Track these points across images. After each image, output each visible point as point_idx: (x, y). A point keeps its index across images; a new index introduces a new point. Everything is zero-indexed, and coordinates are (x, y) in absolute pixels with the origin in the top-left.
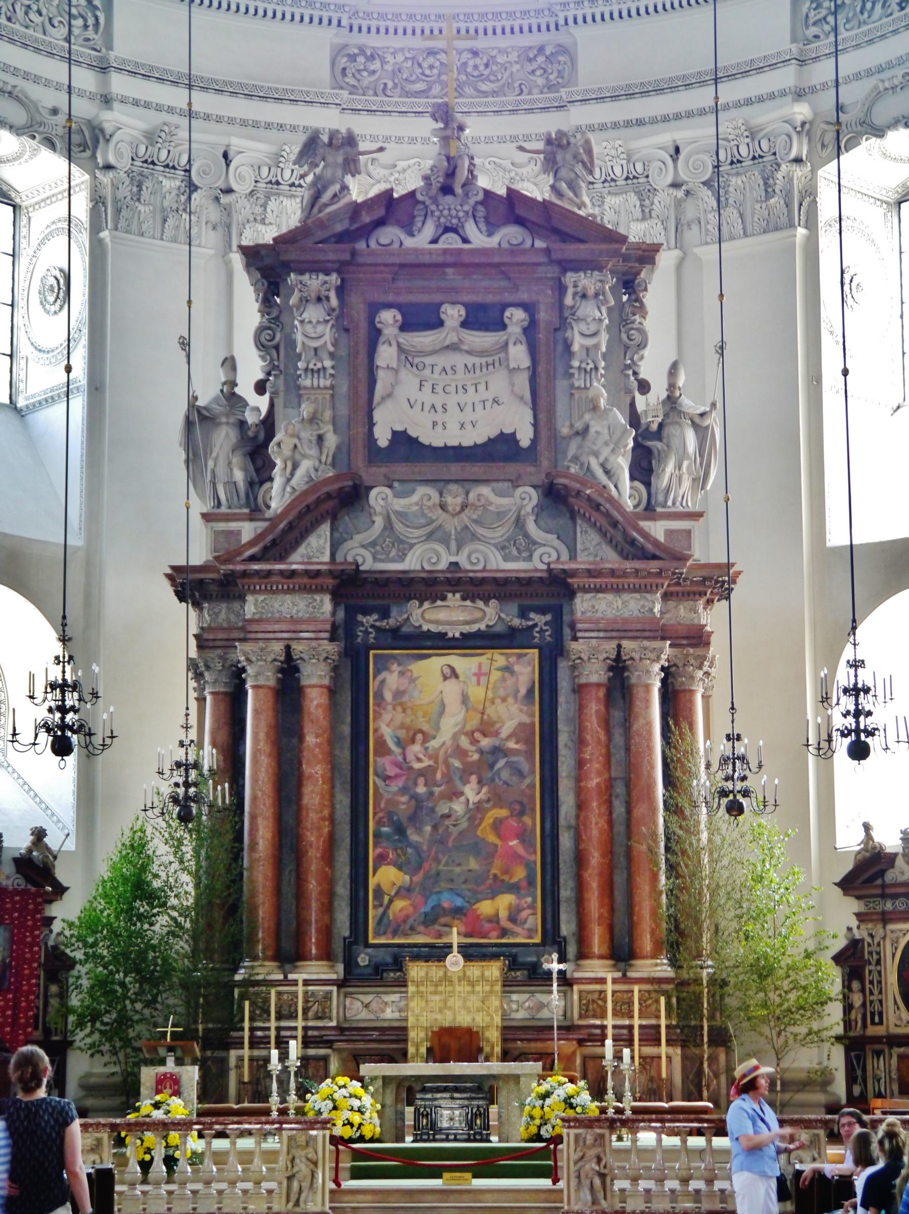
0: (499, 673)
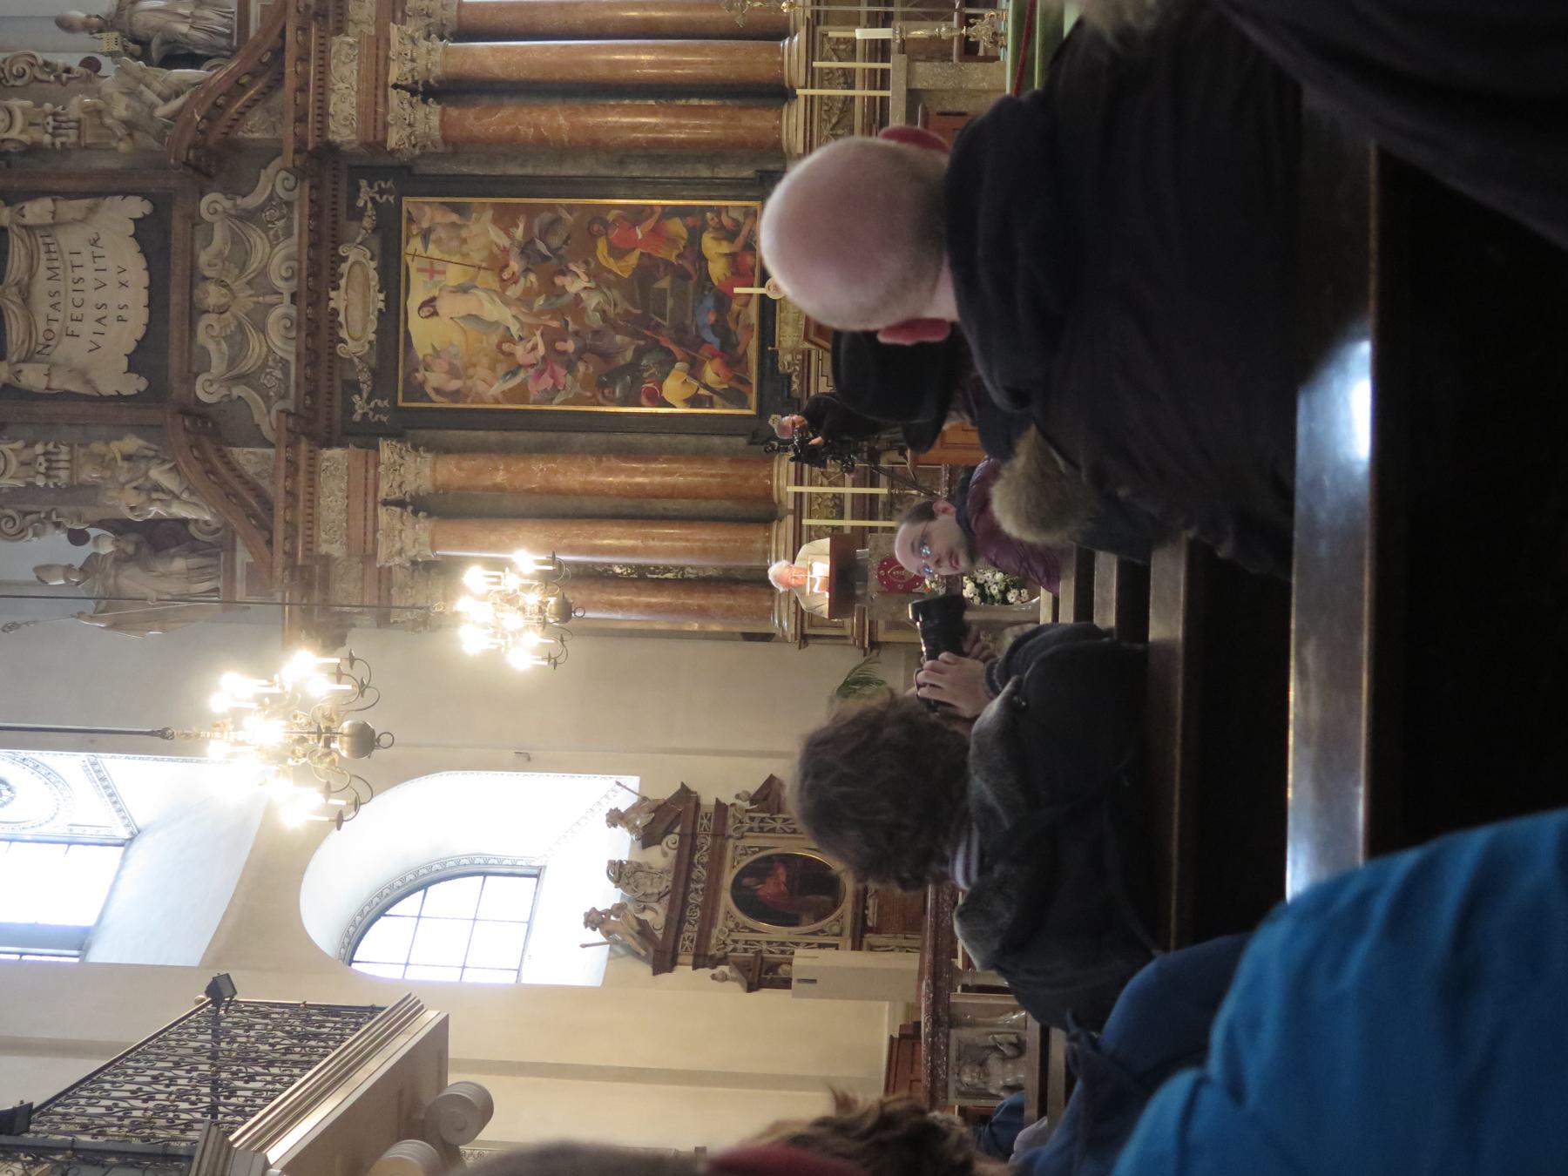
0: (431, 246)
